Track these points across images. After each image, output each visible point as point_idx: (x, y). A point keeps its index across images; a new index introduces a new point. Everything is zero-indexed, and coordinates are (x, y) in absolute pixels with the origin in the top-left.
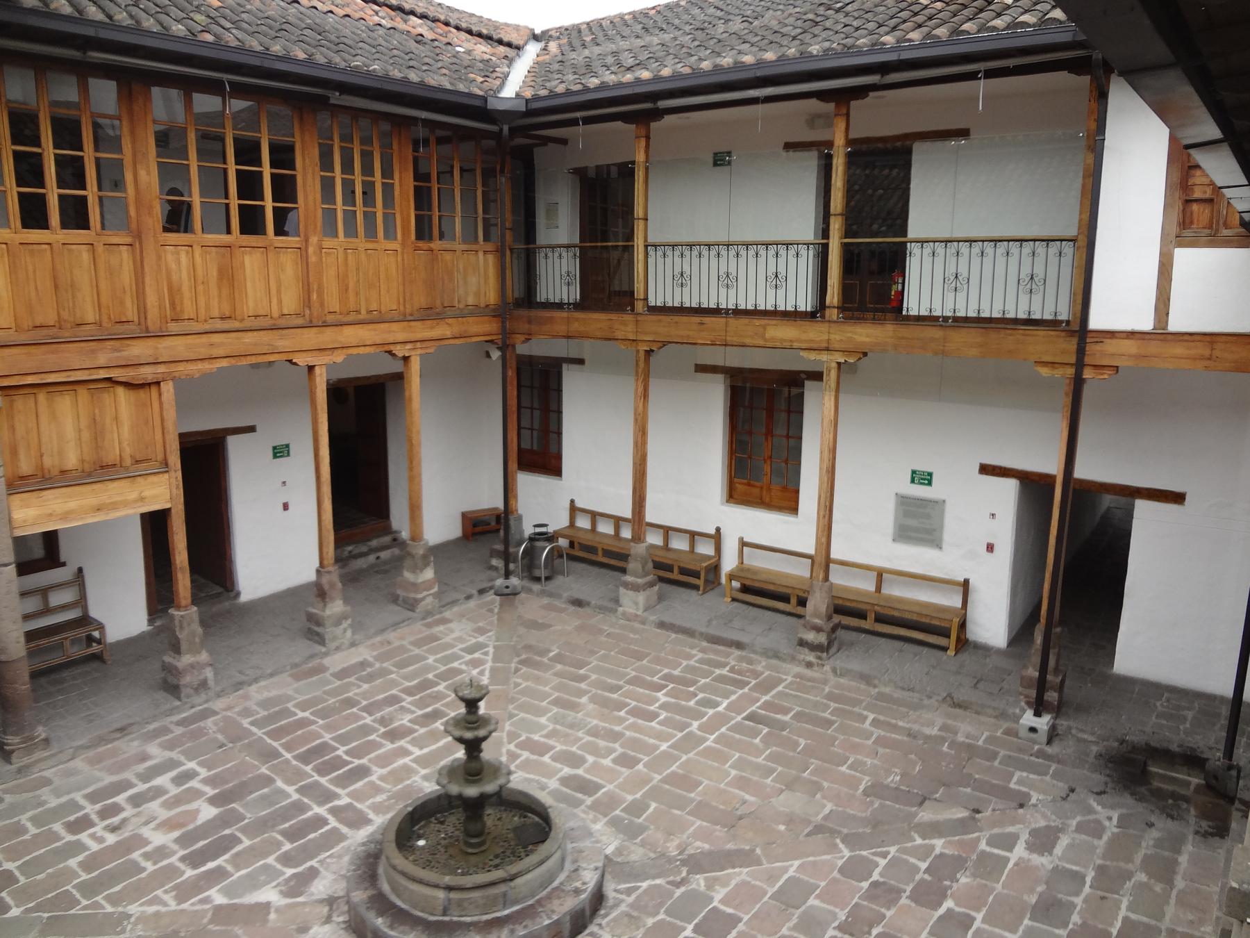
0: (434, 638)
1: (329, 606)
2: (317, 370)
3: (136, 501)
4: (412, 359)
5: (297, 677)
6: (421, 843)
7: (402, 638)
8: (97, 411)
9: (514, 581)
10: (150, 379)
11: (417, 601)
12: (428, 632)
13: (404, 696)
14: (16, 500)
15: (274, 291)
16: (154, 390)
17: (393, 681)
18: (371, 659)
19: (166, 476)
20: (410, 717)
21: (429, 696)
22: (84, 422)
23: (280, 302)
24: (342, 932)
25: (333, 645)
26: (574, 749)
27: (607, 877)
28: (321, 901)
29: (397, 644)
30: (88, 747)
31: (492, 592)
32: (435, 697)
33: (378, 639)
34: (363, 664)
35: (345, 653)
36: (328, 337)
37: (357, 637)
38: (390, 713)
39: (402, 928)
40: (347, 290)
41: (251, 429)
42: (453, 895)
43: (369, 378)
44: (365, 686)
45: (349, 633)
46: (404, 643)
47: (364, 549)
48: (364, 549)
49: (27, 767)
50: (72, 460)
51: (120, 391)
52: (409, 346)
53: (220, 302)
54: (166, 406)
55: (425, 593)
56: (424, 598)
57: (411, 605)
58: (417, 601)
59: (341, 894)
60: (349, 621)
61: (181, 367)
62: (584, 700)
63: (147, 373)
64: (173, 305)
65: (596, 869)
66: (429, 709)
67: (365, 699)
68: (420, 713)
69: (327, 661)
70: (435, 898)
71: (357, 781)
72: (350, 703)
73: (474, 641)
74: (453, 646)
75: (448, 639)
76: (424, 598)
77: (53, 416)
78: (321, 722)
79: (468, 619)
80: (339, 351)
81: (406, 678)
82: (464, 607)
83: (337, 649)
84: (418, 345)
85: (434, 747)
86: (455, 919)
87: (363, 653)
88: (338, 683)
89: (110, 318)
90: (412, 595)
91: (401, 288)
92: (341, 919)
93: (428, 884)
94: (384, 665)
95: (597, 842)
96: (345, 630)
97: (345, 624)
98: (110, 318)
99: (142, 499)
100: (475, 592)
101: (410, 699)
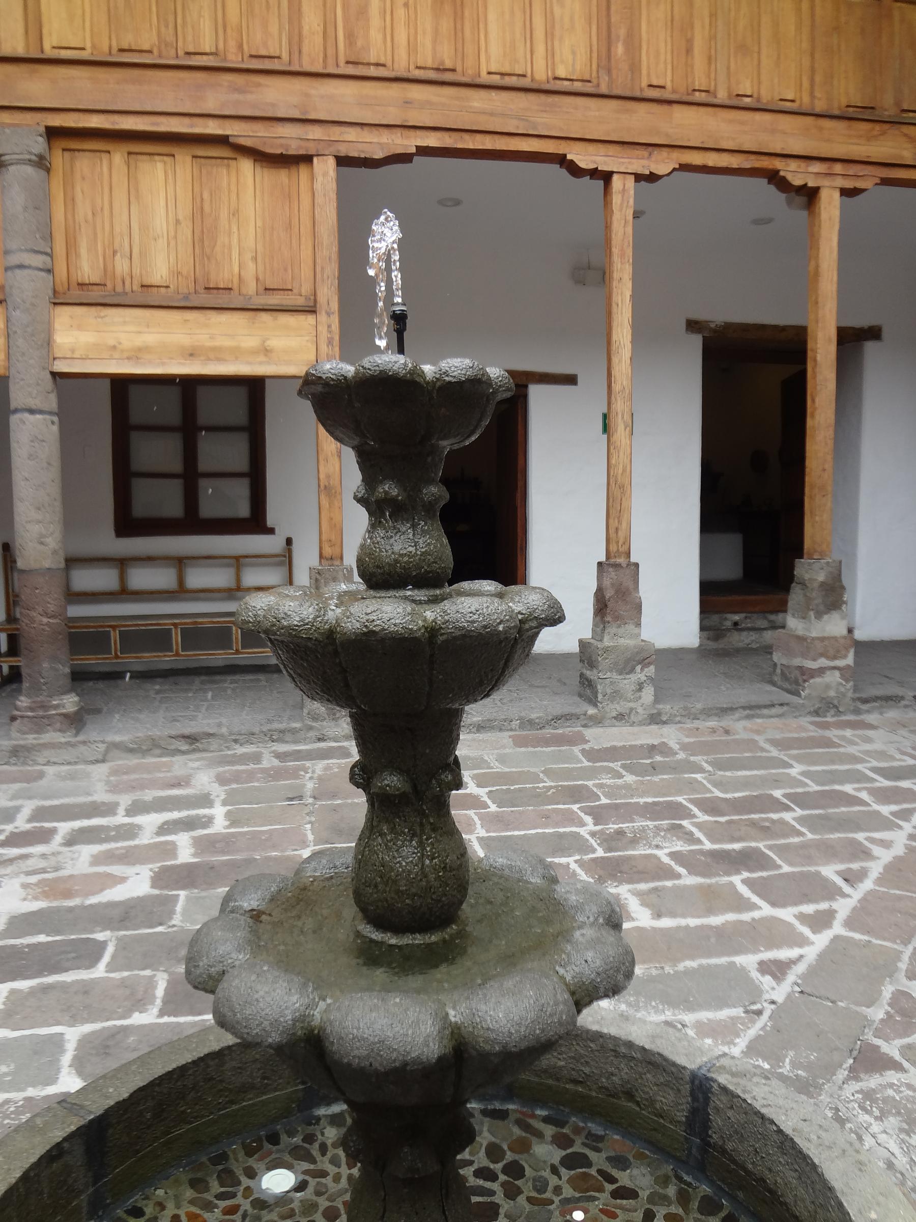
0: (829, 743)
1: (612, 629)
2: (616, 181)
3: (254, 352)
4: (824, 194)
5: (519, 742)
6: (278, 1181)
7: (758, 732)
8: (206, 195)
10: (294, 149)
11: (807, 674)
12: (820, 732)
13: (695, 810)
14: (63, 317)
15: (539, 34)
16: (303, 170)
18: (676, 747)
19: (311, 319)
20: (680, 846)
21: (753, 824)
22: (184, 211)
23: (550, 54)
25: (614, 708)
30: (131, 751)
32: (765, 830)
33: (712, 723)
34: (652, 749)
35: (636, 729)
36: (639, 121)
38: (644, 829)
40: (689, 51)
41: (570, 380)
43: (784, 329)
44: (630, 778)
45: (648, 694)
46: (757, 738)
48: (761, 623)
49: (28, 749)
50: (160, 269)
51: (246, 166)
52: (816, 167)
53: (434, 42)
54: (319, 200)
55: (823, 662)
56: (821, 671)
57: (794, 681)
58: (807, 674)
61: (351, 134)
63: (288, 138)
64: (350, 37)
66: (737, 846)
68: (708, 845)
69: (589, 733)
72: (576, 794)
74: (861, 761)
75: (852, 750)
76: (821, 671)
77: (134, 192)
78: (493, 808)
80: (664, 153)
81: (718, 784)
84: (838, 168)
85: (693, 922)
88: (586, 763)
89: (240, 46)
90: (797, 662)
91: (806, 62)
94: (692, 758)
96: (640, 687)
97: (640, 675)
98: (240, 46)
99: (267, 351)
101: (703, 817)
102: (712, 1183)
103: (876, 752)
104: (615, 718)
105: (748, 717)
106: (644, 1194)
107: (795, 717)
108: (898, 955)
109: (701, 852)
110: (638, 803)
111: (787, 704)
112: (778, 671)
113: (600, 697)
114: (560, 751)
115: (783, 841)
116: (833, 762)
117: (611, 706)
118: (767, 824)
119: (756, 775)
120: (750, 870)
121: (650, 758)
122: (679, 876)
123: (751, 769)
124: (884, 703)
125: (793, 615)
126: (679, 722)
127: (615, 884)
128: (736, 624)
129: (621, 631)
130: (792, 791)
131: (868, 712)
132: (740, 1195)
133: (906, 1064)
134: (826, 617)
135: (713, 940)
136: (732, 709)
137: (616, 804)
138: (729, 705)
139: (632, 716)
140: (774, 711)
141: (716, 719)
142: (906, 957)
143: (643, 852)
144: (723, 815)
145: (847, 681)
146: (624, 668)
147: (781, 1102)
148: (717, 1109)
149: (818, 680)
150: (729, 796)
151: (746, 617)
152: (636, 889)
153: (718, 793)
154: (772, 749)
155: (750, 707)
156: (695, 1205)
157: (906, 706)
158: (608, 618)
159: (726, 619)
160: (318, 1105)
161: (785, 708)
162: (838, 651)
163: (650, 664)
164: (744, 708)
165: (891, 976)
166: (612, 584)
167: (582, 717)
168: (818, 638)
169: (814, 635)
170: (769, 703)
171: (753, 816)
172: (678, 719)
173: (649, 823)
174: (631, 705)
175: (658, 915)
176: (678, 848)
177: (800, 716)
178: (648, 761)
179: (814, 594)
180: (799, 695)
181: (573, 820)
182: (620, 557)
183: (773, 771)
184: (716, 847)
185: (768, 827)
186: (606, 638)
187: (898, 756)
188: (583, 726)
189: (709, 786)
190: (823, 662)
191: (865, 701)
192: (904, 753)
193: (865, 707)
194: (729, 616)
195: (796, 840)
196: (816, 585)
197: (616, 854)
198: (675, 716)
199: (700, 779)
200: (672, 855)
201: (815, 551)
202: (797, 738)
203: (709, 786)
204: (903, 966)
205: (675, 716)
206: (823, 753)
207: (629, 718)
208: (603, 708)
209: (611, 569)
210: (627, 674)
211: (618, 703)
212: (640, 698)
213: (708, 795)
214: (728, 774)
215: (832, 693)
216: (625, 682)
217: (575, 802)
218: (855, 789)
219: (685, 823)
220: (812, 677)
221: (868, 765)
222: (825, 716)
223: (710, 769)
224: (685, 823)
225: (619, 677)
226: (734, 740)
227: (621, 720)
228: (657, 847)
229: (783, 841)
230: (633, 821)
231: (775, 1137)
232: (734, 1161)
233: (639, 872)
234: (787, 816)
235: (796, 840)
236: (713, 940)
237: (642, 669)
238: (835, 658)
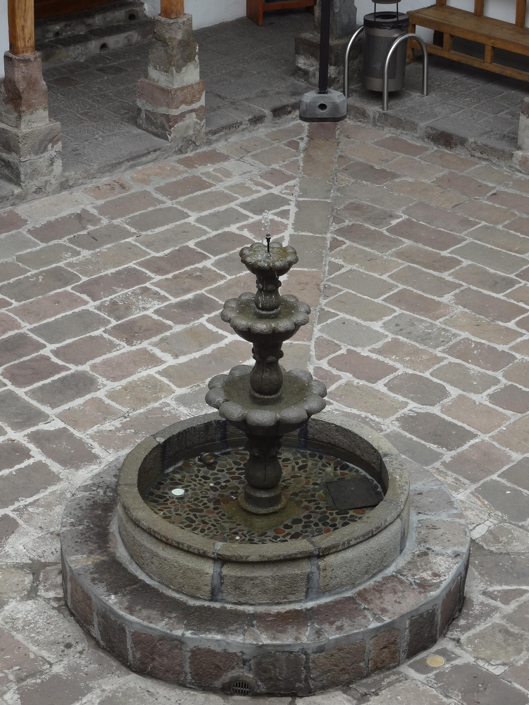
0: (199, 184)
1: (26, 118)
6: (178, 492)
7: (145, 181)
9: (335, 96)
11: (171, 120)
17: (130, 247)
18: (95, 212)
21: (189, 275)
24: (54, 613)
25: (32, 184)
26: (427, 374)
27: (473, 571)
28: (21, 567)
29: (136, 188)
31: (297, 113)
33: (106, 179)
34: (82, 218)
35: (52, 199)
37: (71, 174)
39: (145, 612)
42: (227, 571)
44: (86, 253)
46: (148, 188)
47: (81, 30)
48: (81, 30)
55: (184, 108)
56: (183, 115)
57: (160, 127)
58: (171, 120)
59: (51, 559)
60: (59, 146)
62: (447, 298)
65: (457, 555)
66: (189, 296)
67: (85, 274)
68: (174, 300)
69: (22, 210)
70: (201, 573)
71: (73, 398)
72: (61, 277)
73: (264, 192)
75: (219, 187)
76: (183, 115)
78: (15, 304)
79: (254, 157)
81: (149, 245)
82: (248, 135)
83: (39, 190)
85: (197, 355)
86: (229, 606)
87: (81, 200)
88: (43, 245)
90: (162, 110)
92: (51, 594)
93: (189, 551)
94: (117, 222)
95: (461, 516)
96: (52, 161)
97: (52, 151)
100: (267, 112)
101: (158, 278)
102: (309, 450)
103: (237, 185)
104: (35, 192)
105: (132, 167)
106: (292, 458)
107: (166, 158)
108: (308, 347)
109: (171, 306)
110: (106, 275)
111: (159, 149)
112: (143, 115)
113: (23, 177)
114: (12, 235)
115: (214, 286)
116: (213, 204)
117: (32, 183)
118: (198, 274)
119: (168, 229)
120: (209, 313)
121: (84, 228)
122: (170, 328)
123: (162, 224)
124: (227, 131)
125: (155, 68)
126: (82, 184)
127: (139, 342)
128: (57, 34)
129: (34, 117)
130: (199, 239)
131: (217, 141)
132: (321, 450)
133: (331, 401)
134: (184, 69)
135: (213, 363)
136: (120, 163)
137: (94, 280)
138: (118, 161)
139: (47, 188)
140: (150, 157)
141: (108, 174)
142: (312, 347)
143: (139, 315)
144: (167, 273)
145: (201, 120)
146: (39, 149)
147: (333, 418)
148: (311, 427)
149: (180, 124)
150: (161, 254)
151: (66, 26)
152: (152, 342)
153: (154, 254)
154: (164, 199)
155: (133, 159)
156: (308, 456)
157: (243, 130)
158: (24, 108)
159: (48, 31)
160: (165, 470)
161: (158, 153)
162: (194, 96)
163: (58, 140)
164: (128, 160)
165: (309, 361)
166: (24, 78)
167: (11, 197)
168: (178, 89)
169: (176, 86)
170: (146, 151)
171: (188, 268)
172: (81, 181)
173: (126, 291)
174: (46, 178)
175: (176, 356)
176: (157, 307)
177: (168, 156)
178: (85, 232)
179: (174, 51)
180: (167, 139)
181: (76, 300)
182: (27, 51)
183: (178, 223)
184: (178, 299)
185: (200, 276)
186: (23, 126)
187: (255, 188)
188: (12, 205)
189: (144, 248)
190: (184, 108)
191: (214, 133)
192: (257, 184)
193: (214, 138)
194: (50, 27)
195: (222, 282)
196: (175, 43)
197: (124, 320)
198: (79, 179)
199: (134, 243)
200: (157, 312)
201: (172, 11)
202: (176, 182)
203: (144, 248)
204: (313, 353)
205: (79, 179)
206: (201, 195)
207: (45, 189)
208: (25, 186)
209: (22, 65)
210: (42, 153)
211: (37, 179)
212: (52, 170)
213: (148, 257)
214: (149, 232)
215: (191, 132)
216: (41, 160)
217: (66, 284)
218: (238, 228)
219: (148, 285)
220: (176, 122)
221: (238, 202)
222: (187, 152)
223: (133, 230)
224: (148, 285)
225: (36, 157)
226: (133, 195)
227: (40, 192)
228: (145, 309)
229: (214, 286)
230: (115, 292)
231: (335, 428)
232: (319, 441)
233: (146, 330)
234: (208, 263)
235: (222, 282)
236: (213, 363)
237: (52, 147)
238: (192, 102)
